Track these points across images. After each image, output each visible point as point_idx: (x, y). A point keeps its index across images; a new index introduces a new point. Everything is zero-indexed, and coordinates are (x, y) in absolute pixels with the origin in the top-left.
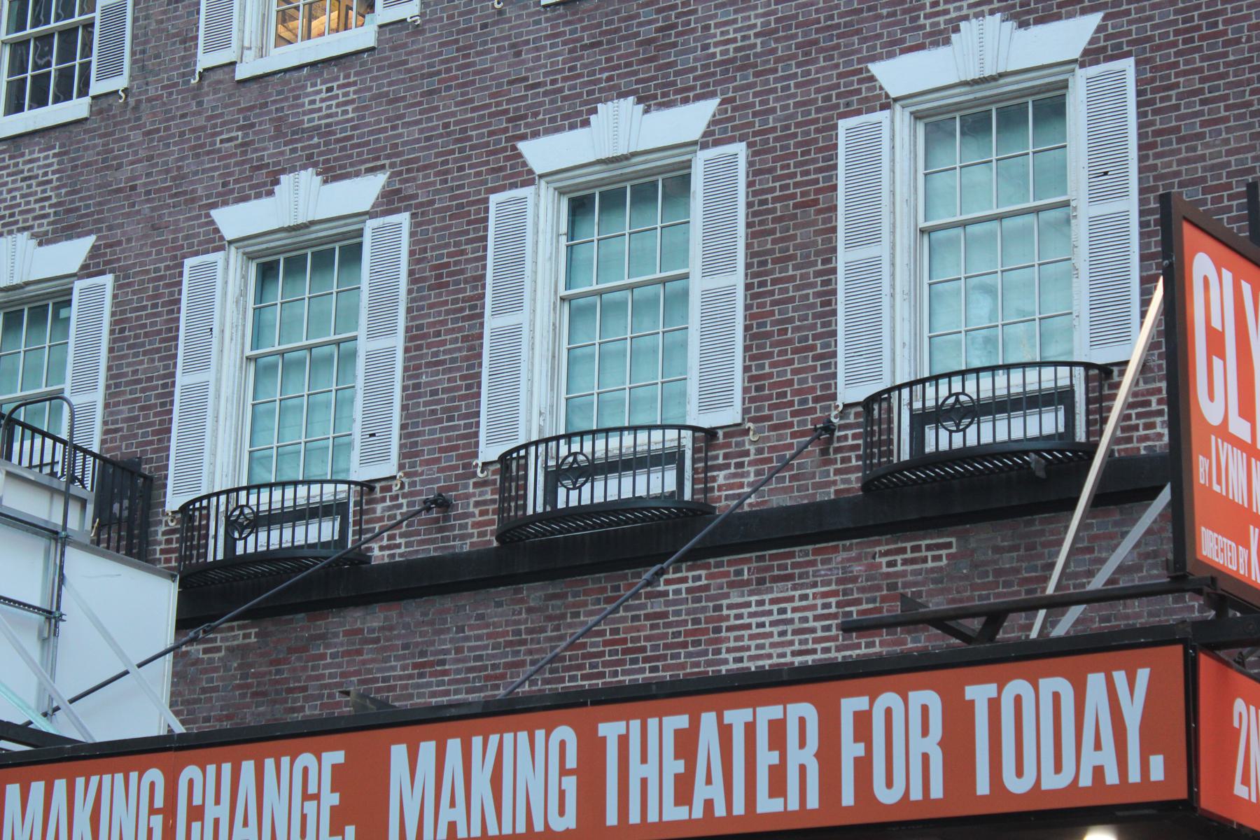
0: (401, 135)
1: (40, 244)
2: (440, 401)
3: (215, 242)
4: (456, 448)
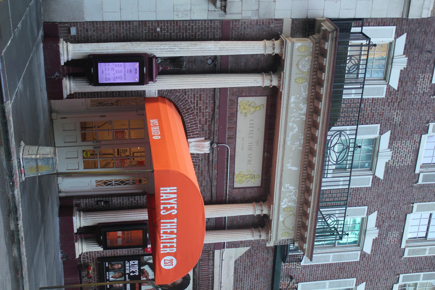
0: (377, 256)
1: (386, 163)
2: (314, 272)
3: (369, 212)
4: (303, 277)
